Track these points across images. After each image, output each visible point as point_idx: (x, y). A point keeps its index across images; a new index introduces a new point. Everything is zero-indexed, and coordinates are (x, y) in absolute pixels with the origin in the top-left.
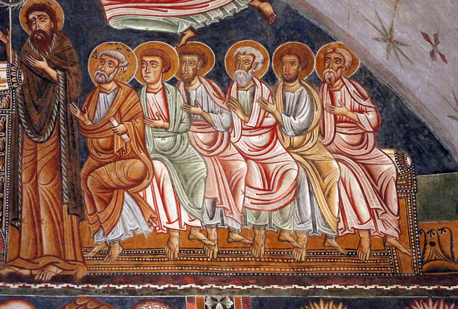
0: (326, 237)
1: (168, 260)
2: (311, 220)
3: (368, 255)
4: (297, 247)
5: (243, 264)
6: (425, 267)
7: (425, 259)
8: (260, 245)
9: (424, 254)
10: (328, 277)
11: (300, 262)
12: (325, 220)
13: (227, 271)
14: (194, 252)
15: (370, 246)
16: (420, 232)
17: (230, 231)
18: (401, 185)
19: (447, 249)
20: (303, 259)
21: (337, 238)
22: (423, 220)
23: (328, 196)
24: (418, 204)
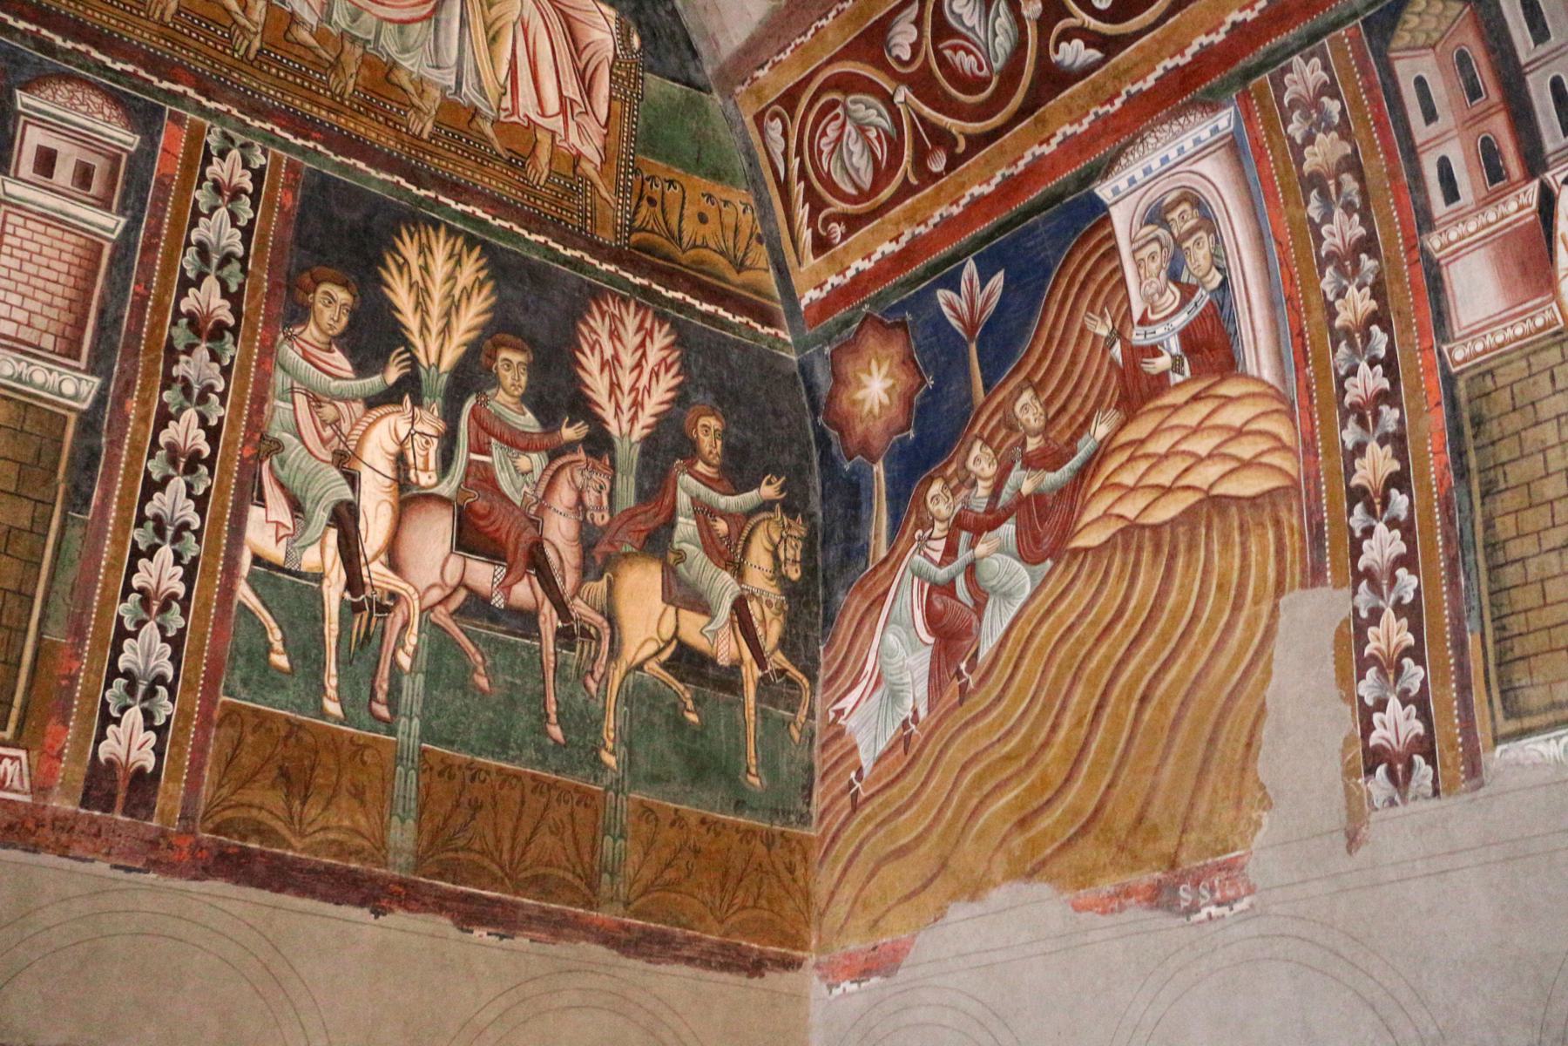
0: (476, 112)
1: (147, 18)
2: (454, 70)
3: (544, 177)
4: (419, 109)
5: (305, 93)
6: (634, 238)
7: (637, 224)
8: (348, 72)
9: (635, 213)
10: (466, 189)
11: (419, 137)
12: (480, 80)
13: (270, 95)
14: (208, 27)
15: (550, 162)
16: (636, 172)
17: (293, 18)
18: (618, 76)
19: (674, 221)
20: (425, 136)
21: (496, 122)
22: (644, 152)
23: (493, 40)
24: (641, 122)
